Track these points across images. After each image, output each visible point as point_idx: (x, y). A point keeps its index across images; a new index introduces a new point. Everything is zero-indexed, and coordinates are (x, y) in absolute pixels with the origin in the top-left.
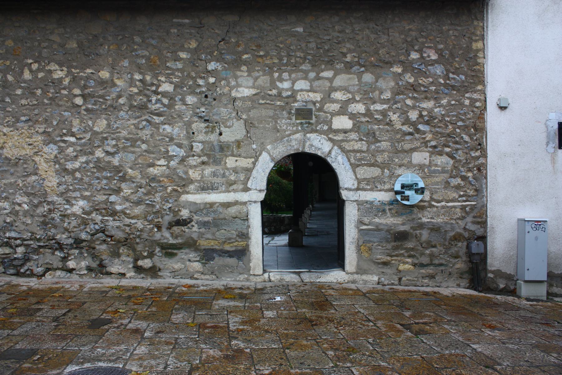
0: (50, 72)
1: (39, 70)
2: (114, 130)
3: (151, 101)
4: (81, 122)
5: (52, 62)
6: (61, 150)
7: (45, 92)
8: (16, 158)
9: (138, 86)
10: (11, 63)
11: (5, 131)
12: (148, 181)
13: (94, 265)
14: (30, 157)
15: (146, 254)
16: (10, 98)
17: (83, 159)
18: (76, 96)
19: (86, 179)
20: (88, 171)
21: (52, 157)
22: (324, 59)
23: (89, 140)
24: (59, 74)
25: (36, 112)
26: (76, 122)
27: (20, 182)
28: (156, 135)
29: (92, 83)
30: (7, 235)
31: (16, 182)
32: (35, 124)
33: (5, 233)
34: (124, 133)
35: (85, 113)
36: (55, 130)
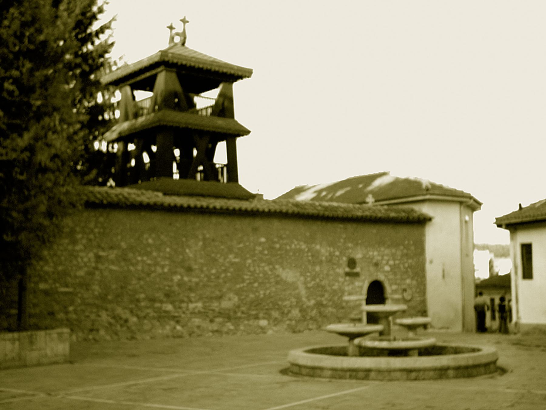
6: (306, 279)
17: (313, 283)
22: (381, 243)
24: (304, 246)
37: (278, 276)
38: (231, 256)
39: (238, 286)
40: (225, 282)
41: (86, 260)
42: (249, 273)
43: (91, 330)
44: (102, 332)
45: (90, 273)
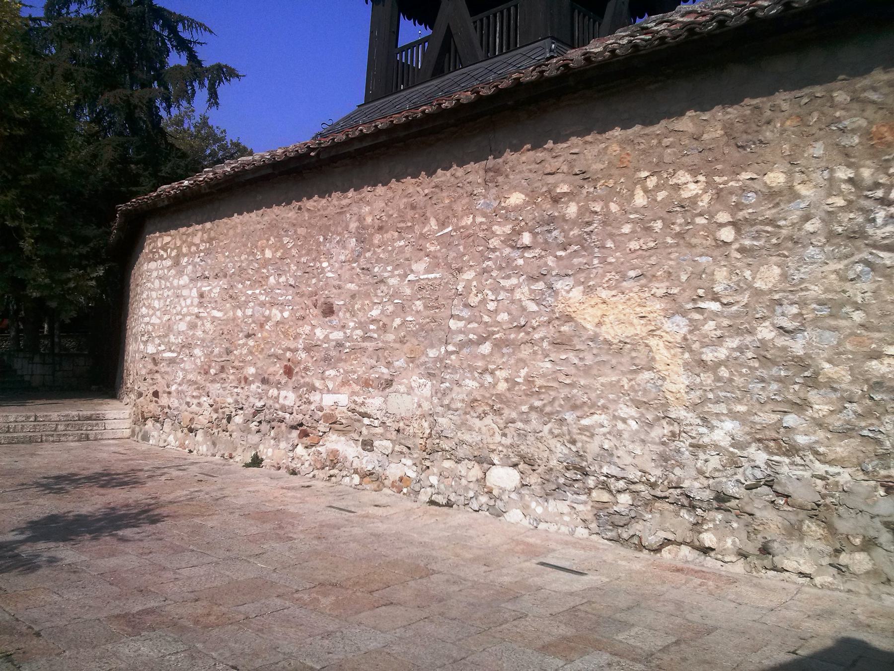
0: (677, 187)
1: (658, 188)
2: (794, 285)
3: (874, 220)
4: (731, 273)
5: (680, 169)
6: (694, 327)
7: (668, 224)
8: (620, 341)
9: (846, 192)
10: (615, 183)
11: (604, 296)
12: (865, 388)
13: (751, 548)
14: (642, 338)
15: (858, 541)
16: (614, 241)
18: (721, 225)
19: (739, 381)
20: (742, 365)
21: (679, 338)
23: (745, 306)
24: (692, 187)
25: (653, 260)
26: (721, 274)
27: (624, 381)
28: (884, 292)
29: (752, 198)
30: (605, 470)
31: (619, 381)
32: (650, 281)
33: (601, 467)
34: (815, 291)
35: (739, 256)
36: (684, 290)
37: (569, 319)
38: (419, 267)
39: (432, 353)
40: (402, 341)
41: (189, 301)
42: (466, 313)
43: (191, 430)
44: (200, 436)
45: (193, 326)
